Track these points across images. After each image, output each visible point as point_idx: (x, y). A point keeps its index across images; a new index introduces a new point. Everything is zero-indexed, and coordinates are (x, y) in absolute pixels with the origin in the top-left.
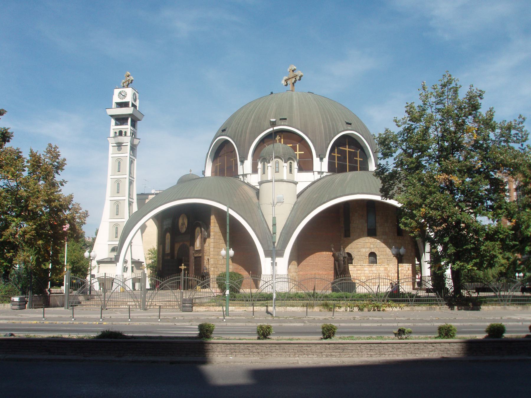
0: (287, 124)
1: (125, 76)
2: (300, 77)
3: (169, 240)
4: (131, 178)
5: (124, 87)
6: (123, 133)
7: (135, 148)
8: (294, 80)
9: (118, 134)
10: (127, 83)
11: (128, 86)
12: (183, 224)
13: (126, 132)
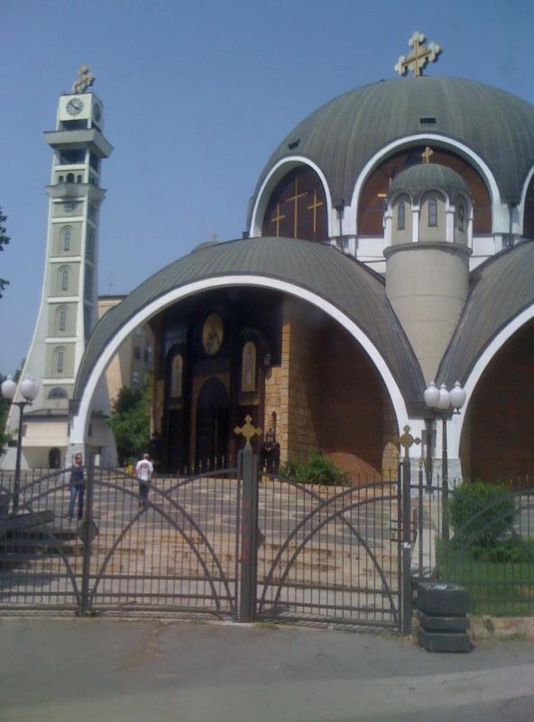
0: (436, 130)
1: (80, 73)
2: (437, 55)
3: (180, 370)
4: (90, 264)
5: (77, 93)
6: (76, 179)
7: (96, 207)
8: (422, 61)
9: (65, 180)
10: (83, 85)
11: (84, 91)
12: (213, 336)
13: (80, 177)
